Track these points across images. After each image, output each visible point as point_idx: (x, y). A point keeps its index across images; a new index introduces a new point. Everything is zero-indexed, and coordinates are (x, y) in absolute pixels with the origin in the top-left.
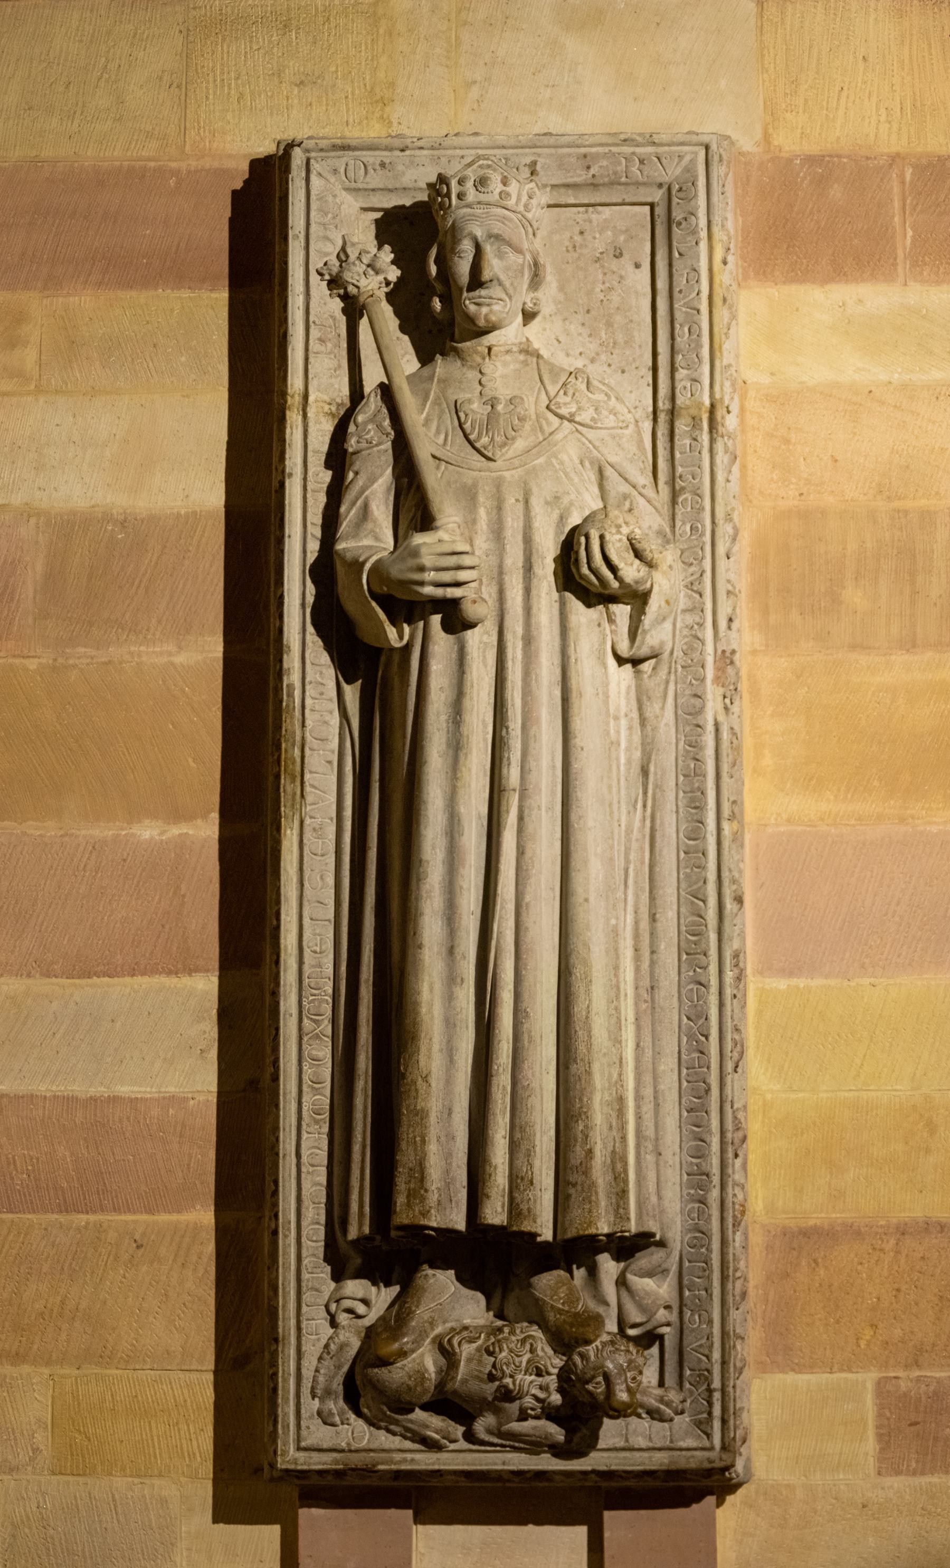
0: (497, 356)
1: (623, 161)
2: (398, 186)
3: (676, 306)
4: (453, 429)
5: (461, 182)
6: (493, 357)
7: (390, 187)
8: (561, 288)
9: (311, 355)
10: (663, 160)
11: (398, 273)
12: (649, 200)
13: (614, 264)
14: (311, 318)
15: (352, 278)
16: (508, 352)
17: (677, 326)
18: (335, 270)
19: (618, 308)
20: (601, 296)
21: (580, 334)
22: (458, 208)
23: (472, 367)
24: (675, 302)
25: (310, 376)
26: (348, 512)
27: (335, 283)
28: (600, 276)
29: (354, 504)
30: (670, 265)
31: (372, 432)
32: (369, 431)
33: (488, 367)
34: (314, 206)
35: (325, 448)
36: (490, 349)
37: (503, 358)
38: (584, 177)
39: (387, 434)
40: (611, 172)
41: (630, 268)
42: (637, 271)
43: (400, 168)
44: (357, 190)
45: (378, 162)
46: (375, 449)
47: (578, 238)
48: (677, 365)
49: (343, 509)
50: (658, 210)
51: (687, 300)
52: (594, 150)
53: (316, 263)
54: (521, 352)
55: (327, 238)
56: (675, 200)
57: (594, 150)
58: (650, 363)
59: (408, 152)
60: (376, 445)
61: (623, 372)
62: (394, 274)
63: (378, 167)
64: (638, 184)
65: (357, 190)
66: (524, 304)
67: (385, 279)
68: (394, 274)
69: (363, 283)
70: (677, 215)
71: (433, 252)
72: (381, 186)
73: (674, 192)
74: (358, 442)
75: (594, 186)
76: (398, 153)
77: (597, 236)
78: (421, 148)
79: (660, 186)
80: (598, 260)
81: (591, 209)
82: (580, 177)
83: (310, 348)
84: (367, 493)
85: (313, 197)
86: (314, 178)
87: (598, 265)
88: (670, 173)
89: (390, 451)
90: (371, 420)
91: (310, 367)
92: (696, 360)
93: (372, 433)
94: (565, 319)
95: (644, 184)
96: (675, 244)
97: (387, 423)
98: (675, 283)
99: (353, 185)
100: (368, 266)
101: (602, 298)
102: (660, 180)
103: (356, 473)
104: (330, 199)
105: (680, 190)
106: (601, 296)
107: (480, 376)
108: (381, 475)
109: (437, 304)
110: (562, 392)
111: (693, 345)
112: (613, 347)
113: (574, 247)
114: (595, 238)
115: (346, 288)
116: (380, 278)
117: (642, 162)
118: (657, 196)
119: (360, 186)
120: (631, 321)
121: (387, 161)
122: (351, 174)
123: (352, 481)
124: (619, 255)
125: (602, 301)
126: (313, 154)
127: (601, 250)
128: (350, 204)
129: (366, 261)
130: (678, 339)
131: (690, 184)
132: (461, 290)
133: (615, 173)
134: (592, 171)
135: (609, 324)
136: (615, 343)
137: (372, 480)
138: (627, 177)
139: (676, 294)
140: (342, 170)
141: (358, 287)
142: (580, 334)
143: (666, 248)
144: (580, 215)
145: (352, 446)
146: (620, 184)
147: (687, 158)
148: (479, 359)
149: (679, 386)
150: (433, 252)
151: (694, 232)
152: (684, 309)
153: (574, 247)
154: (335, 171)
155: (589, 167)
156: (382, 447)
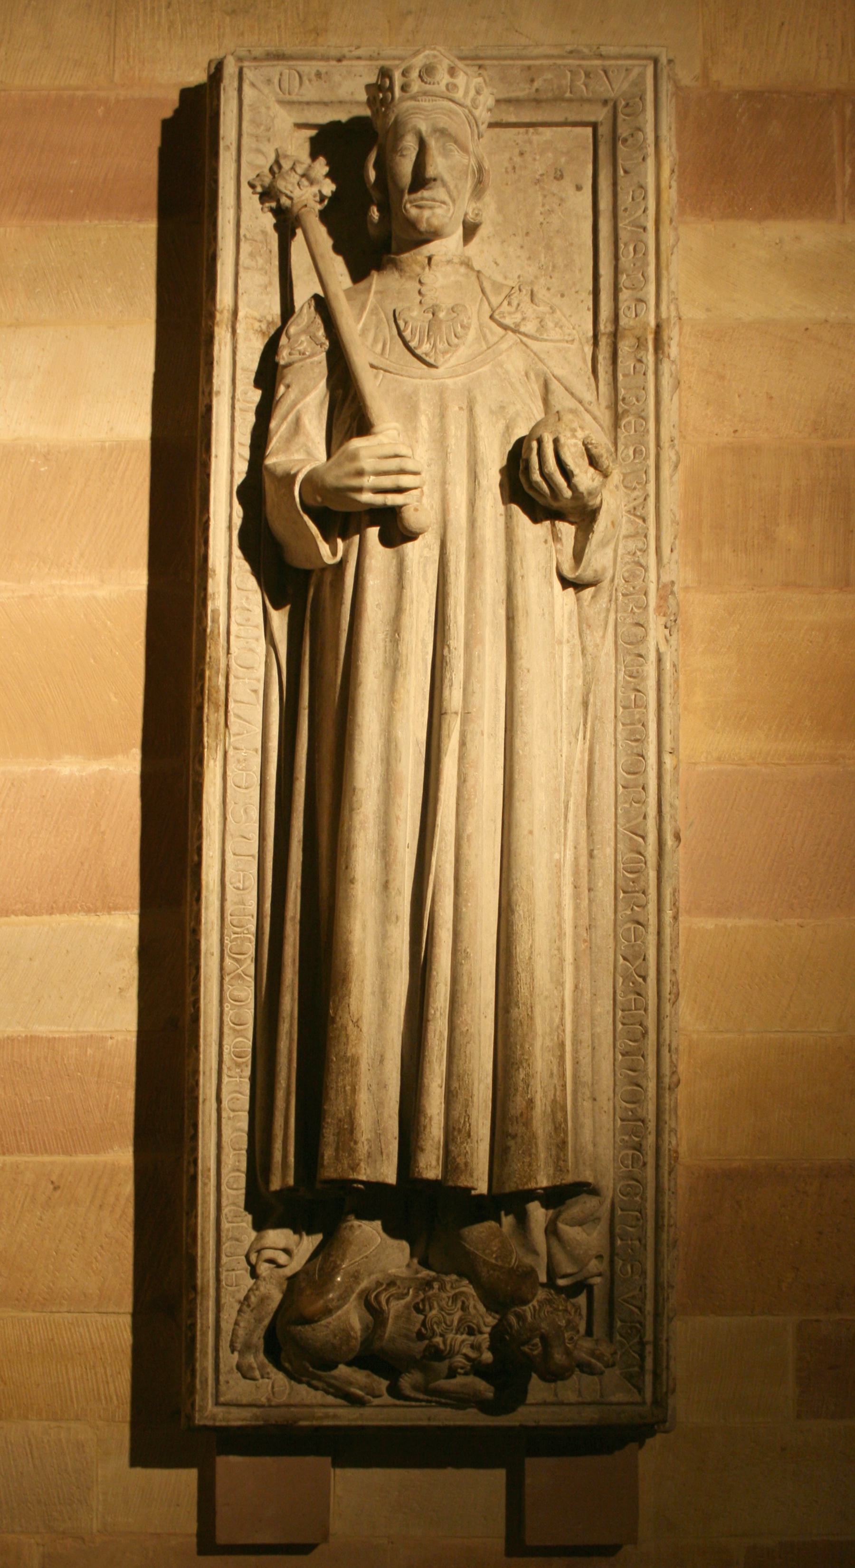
0: (437, 265)
1: (569, 74)
2: (334, 98)
3: (621, 225)
4: (392, 338)
5: (404, 74)
6: (433, 267)
7: (326, 99)
8: (500, 210)
9: (241, 270)
10: (610, 74)
11: (333, 187)
12: (592, 119)
13: (554, 187)
14: (242, 232)
15: (286, 187)
16: (449, 262)
17: (622, 246)
18: (267, 180)
19: (558, 231)
20: (541, 219)
21: (519, 257)
22: (402, 99)
23: (411, 278)
24: (619, 220)
25: (240, 291)
26: (279, 427)
27: (267, 194)
28: (540, 199)
29: (285, 418)
30: (615, 184)
31: (304, 343)
32: (302, 342)
33: (428, 276)
34: (246, 116)
35: (255, 366)
36: (430, 259)
37: (443, 269)
38: (527, 92)
39: (321, 345)
40: (555, 86)
41: (571, 190)
42: (578, 193)
43: (337, 78)
44: (291, 103)
45: (313, 72)
46: (308, 361)
47: (517, 159)
48: (621, 285)
49: (273, 425)
50: (601, 130)
51: (632, 218)
52: (538, 62)
53: (248, 174)
54: (462, 263)
55: (259, 151)
56: (621, 117)
57: (538, 62)
58: (590, 287)
59: (345, 63)
60: (310, 357)
61: (562, 296)
62: (329, 188)
63: (313, 77)
64: (583, 100)
65: (291, 103)
66: (466, 214)
67: (320, 192)
68: (329, 188)
69: (297, 193)
70: (623, 131)
71: (372, 157)
72: (316, 98)
73: (620, 109)
74: (290, 354)
75: (537, 101)
76: (334, 63)
77: (538, 157)
78: (359, 58)
79: (605, 102)
80: (538, 182)
81: (531, 130)
82: (522, 91)
83: (241, 262)
84: (299, 407)
85: (245, 108)
86: (246, 87)
87: (537, 187)
88: (616, 89)
89: (325, 363)
90: (305, 331)
91: (240, 282)
92: (642, 279)
93: (305, 344)
94: (503, 242)
95: (589, 100)
96: (620, 161)
97: (321, 333)
98: (619, 202)
99: (287, 97)
100: (303, 176)
101: (541, 220)
102: (606, 96)
103: (288, 387)
104: (263, 110)
105: (627, 105)
106: (541, 219)
107: (419, 286)
108: (315, 387)
109: (375, 213)
110: (506, 303)
111: (638, 264)
112: (553, 271)
113: (514, 168)
114: (535, 159)
115: (278, 201)
116: (315, 189)
117: (587, 75)
118: (601, 114)
119: (294, 98)
120: (571, 245)
121: (323, 71)
122: (285, 85)
123: (283, 395)
124: (559, 177)
125: (541, 224)
126: (246, 64)
127: (540, 172)
128: (284, 119)
129: (300, 170)
130: (622, 259)
131: (637, 99)
132: (402, 192)
133: (560, 87)
134: (536, 85)
135: (549, 248)
136: (554, 267)
137: (304, 393)
138: (571, 92)
139: (621, 213)
140: (276, 81)
141: (291, 198)
142: (519, 257)
143: (611, 169)
144: (520, 136)
145: (283, 358)
146: (564, 100)
147: (635, 72)
148: (418, 269)
149: (623, 307)
150: (372, 157)
151: (641, 148)
152: (629, 228)
153: (514, 168)
154: (269, 81)
155: (532, 81)
156: (316, 359)
